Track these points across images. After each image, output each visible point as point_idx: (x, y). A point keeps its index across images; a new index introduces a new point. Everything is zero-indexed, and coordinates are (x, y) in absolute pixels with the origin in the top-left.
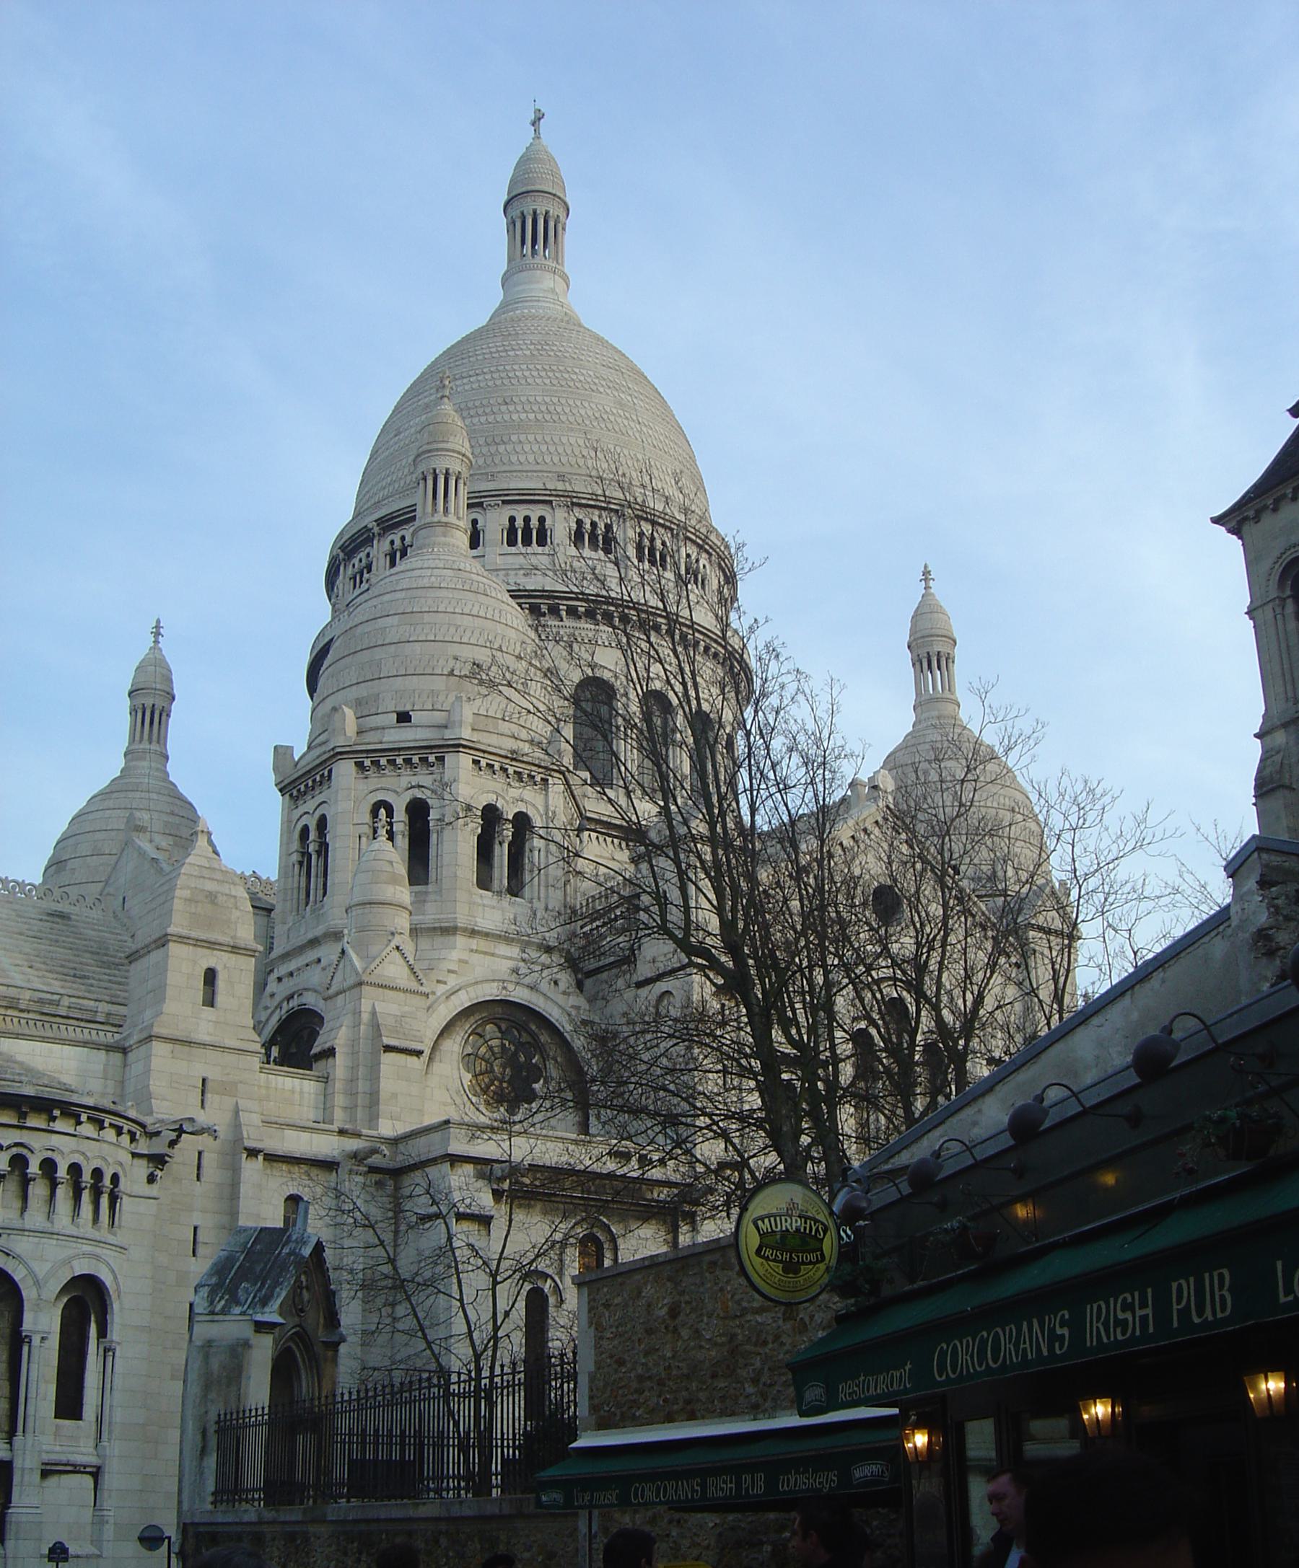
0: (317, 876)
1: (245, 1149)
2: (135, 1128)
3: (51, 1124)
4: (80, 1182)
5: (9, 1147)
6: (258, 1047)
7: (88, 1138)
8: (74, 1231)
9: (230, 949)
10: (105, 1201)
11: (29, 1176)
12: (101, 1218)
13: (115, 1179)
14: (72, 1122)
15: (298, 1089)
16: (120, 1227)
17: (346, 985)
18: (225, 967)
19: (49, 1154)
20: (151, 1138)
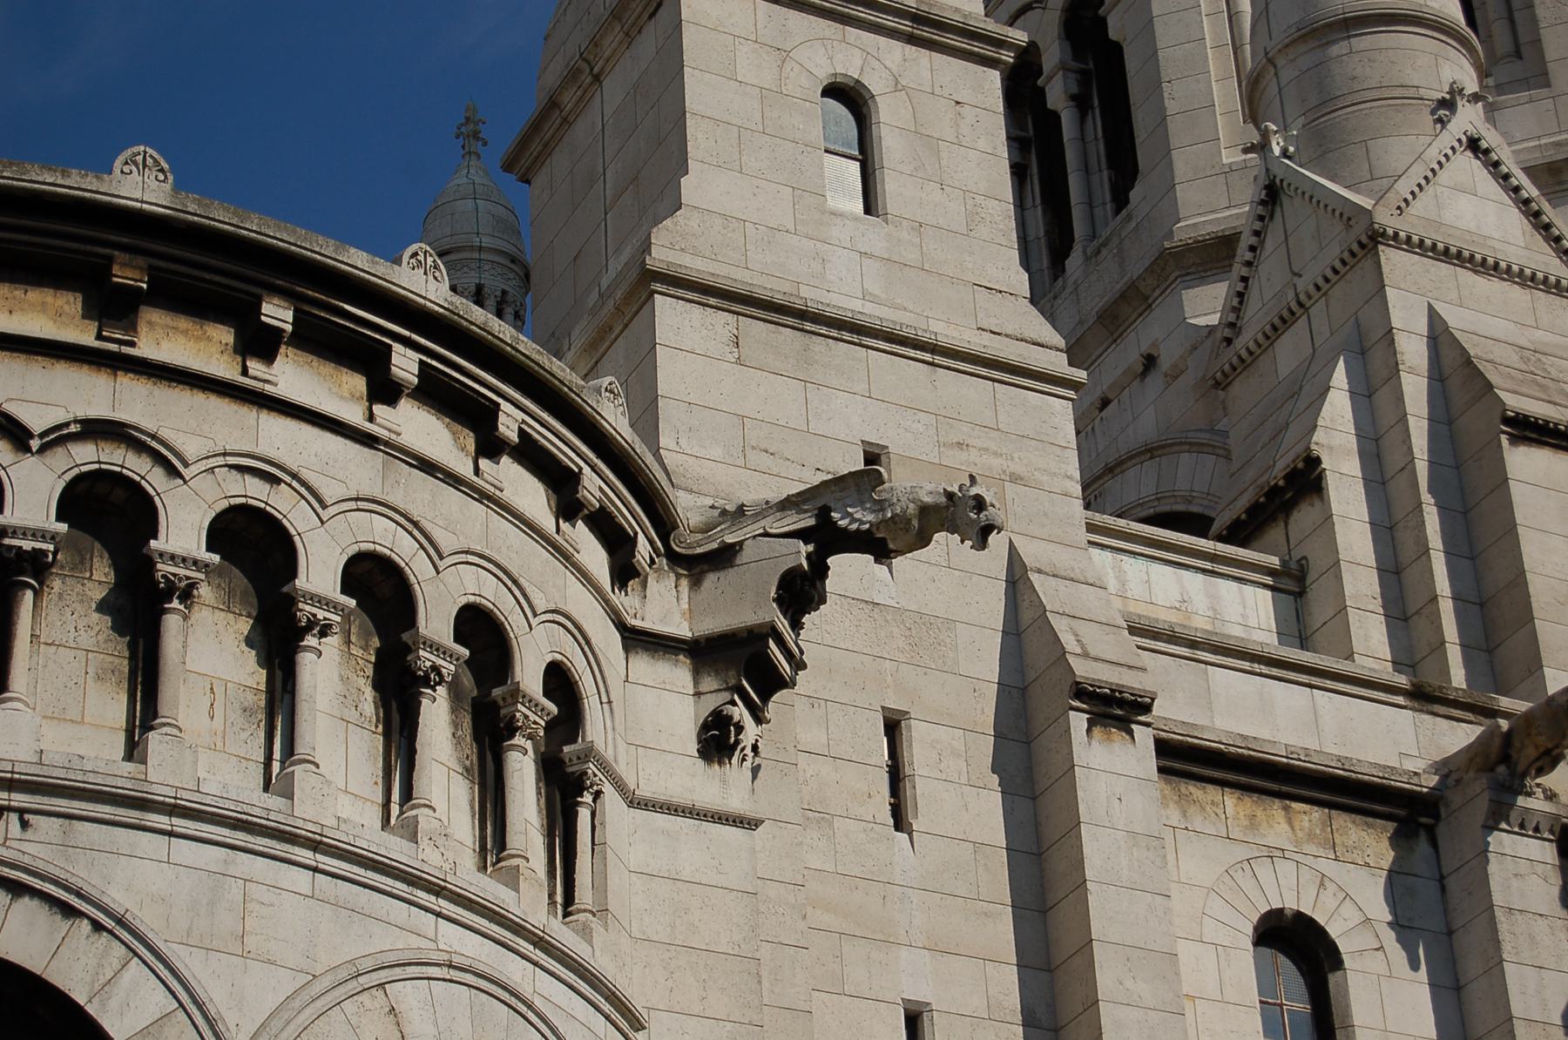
0: (1086, 169)
1: (1083, 693)
2: (629, 513)
3: (255, 366)
4: (407, 649)
5: (57, 438)
6: (1058, 363)
7: (428, 467)
8: (394, 848)
9: (905, 26)
10: (522, 770)
11: (164, 568)
12: (514, 841)
13: (559, 679)
14: (359, 383)
15: (1200, 603)
16: (602, 911)
17: (1312, 273)
18: (897, 87)
19: (255, 492)
20: (696, 583)
